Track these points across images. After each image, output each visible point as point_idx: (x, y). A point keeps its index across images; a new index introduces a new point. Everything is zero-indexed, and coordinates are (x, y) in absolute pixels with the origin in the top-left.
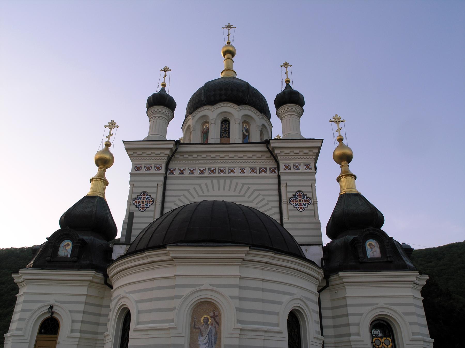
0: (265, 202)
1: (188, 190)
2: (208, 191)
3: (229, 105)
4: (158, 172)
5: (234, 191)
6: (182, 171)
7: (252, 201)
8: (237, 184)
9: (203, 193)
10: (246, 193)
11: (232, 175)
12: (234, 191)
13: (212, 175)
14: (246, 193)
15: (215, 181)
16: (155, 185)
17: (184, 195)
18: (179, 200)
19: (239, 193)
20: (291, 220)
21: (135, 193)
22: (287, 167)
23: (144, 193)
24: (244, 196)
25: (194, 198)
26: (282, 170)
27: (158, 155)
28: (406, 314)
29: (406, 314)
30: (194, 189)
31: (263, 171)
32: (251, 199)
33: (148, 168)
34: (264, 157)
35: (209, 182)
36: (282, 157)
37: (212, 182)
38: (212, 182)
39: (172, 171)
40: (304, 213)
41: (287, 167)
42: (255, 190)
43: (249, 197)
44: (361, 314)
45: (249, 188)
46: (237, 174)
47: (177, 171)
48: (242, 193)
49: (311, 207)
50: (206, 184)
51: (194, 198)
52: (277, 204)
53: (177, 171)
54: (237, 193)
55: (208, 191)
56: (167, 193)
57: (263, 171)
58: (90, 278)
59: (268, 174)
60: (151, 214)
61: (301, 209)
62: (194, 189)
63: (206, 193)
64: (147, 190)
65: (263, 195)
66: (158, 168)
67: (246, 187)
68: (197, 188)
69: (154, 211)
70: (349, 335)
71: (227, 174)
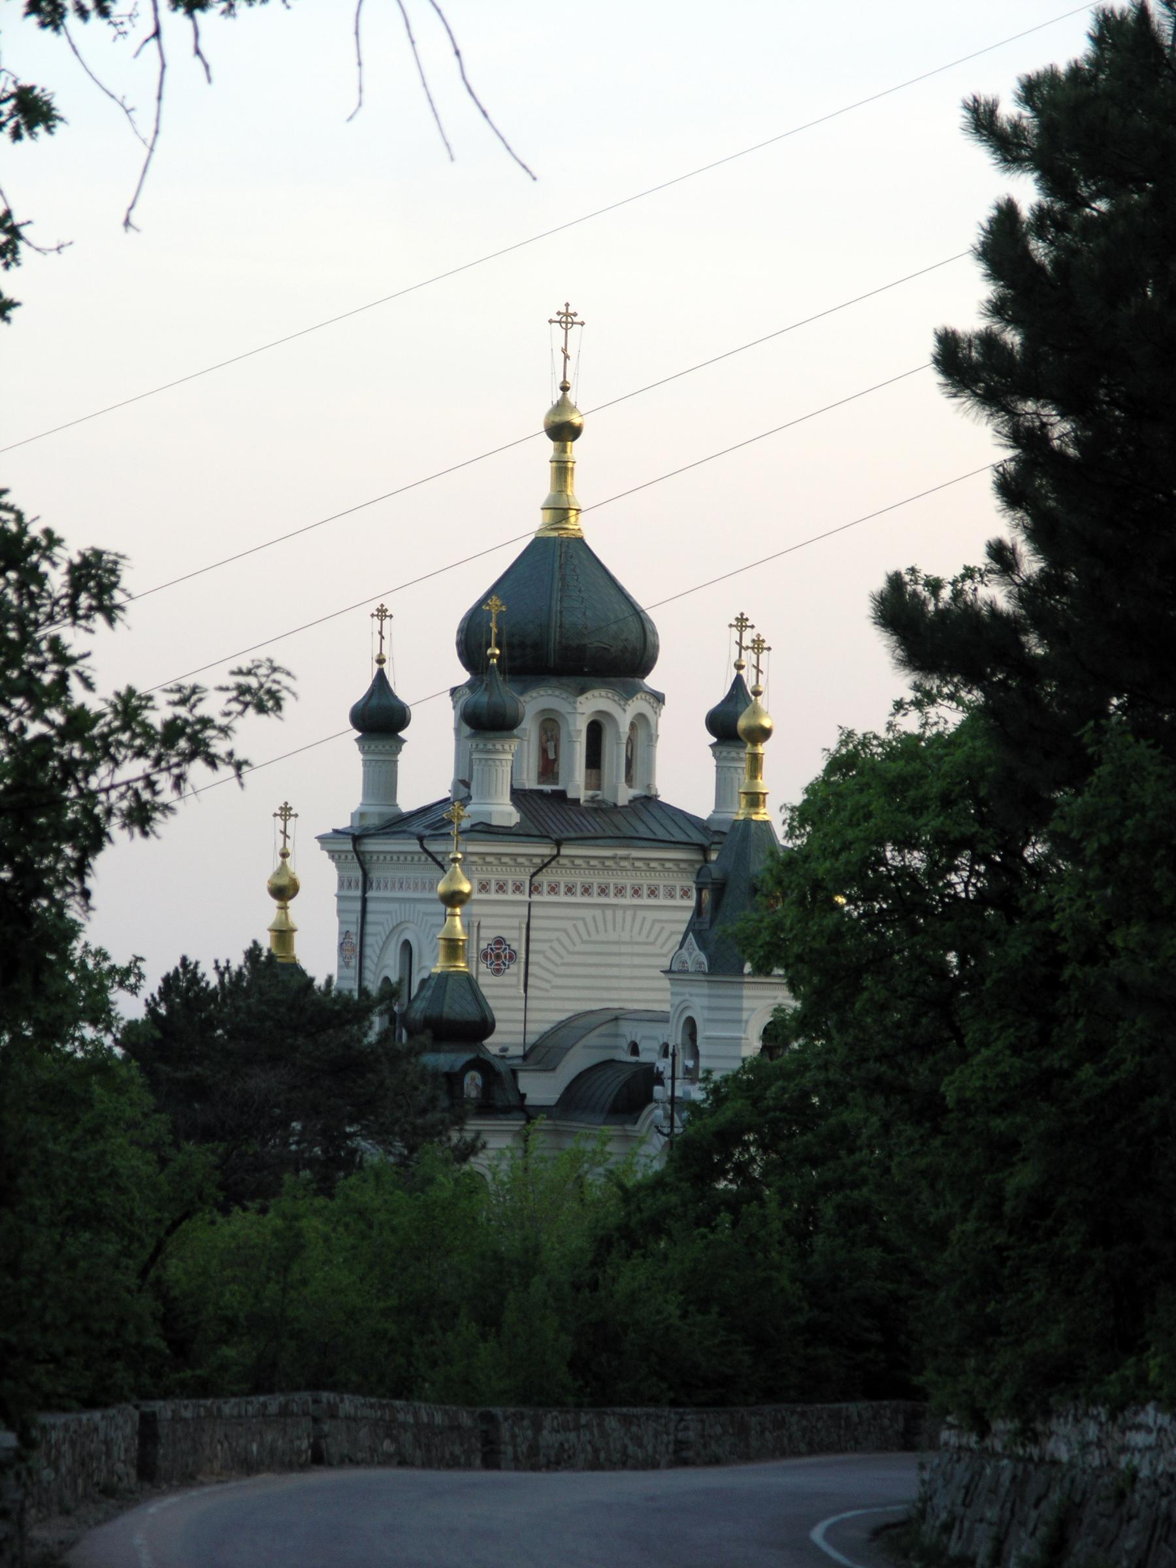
1: (565, 930)
2: (597, 931)
4: (518, 897)
6: (553, 889)
8: (644, 919)
10: (656, 939)
11: (636, 901)
13: (603, 900)
14: (656, 939)
15: (609, 913)
16: (515, 922)
17: (558, 940)
18: (551, 948)
19: (648, 937)
21: (485, 939)
23: (500, 941)
25: (574, 944)
27: (521, 865)
30: (575, 926)
32: (665, 950)
33: (501, 888)
35: (598, 913)
37: (604, 914)
39: (536, 889)
45: (663, 928)
47: (545, 888)
48: (651, 939)
50: (594, 918)
51: (574, 944)
53: (545, 888)
54: (642, 939)
55: (597, 931)
56: (533, 934)
57: (685, 894)
58: (517, 1128)
60: (513, 980)
62: (575, 926)
63: (595, 937)
64: (504, 934)
66: (518, 888)
67: (657, 927)
68: (580, 924)
69: (517, 975)
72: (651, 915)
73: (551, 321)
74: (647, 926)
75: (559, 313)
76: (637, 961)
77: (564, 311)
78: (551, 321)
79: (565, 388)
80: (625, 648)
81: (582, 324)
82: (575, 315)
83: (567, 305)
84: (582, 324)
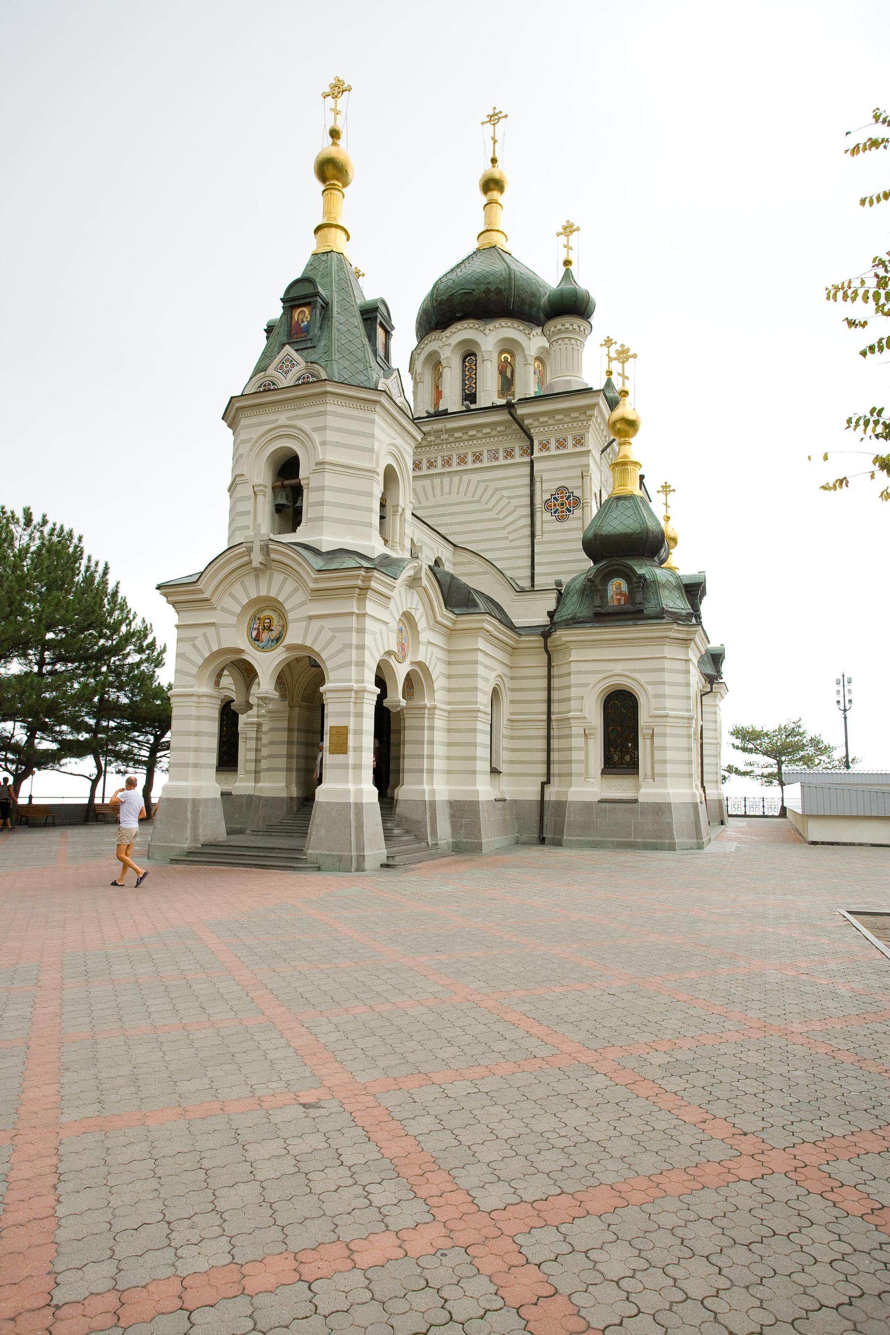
0: (510, 508)
3: (471, 325)
5: (465, 495)
7: (491, 510)
8: (470, 481)
9: (420, 503)
12: (465, 495)
15: (437, 481)
20: (547, 537)
22: (545, 446)
24: (478, 501)
26: (537, 454)
28: (649, 683)
29: (649, 683)
31: (509, 454)
32: (489, 506)
34: (509, 431)
35: (427, 482)
36: (537, 430)
38: (432, 483)
40: (566, 525)
41: (545, 446)
42: (497, 490)
43: (486, 504)
44: (587, 685)
45: (487, 486)
46: (470, 466)
48: (476, 498)
49: (578, 513)
50: (423, 486)
52: (527, 511)
57: (509, 454)
59: (518, 459)
61: (561, 519)
63: (425, 504)
65: (508, 498)
67: (482, 486)
70: (570, 711)
71: (455, 468)
72: (475, 477)
73: (483, 123)
74: (472, 488)
75: (488, 116)
76: (463, 518)
77: (491, 113)
78: (483, 123)
79: (494, 161)
80: (488, 289)
81: (506, 116)
82: (501, 112)
83: (495, 108)
84: (506, 116)
